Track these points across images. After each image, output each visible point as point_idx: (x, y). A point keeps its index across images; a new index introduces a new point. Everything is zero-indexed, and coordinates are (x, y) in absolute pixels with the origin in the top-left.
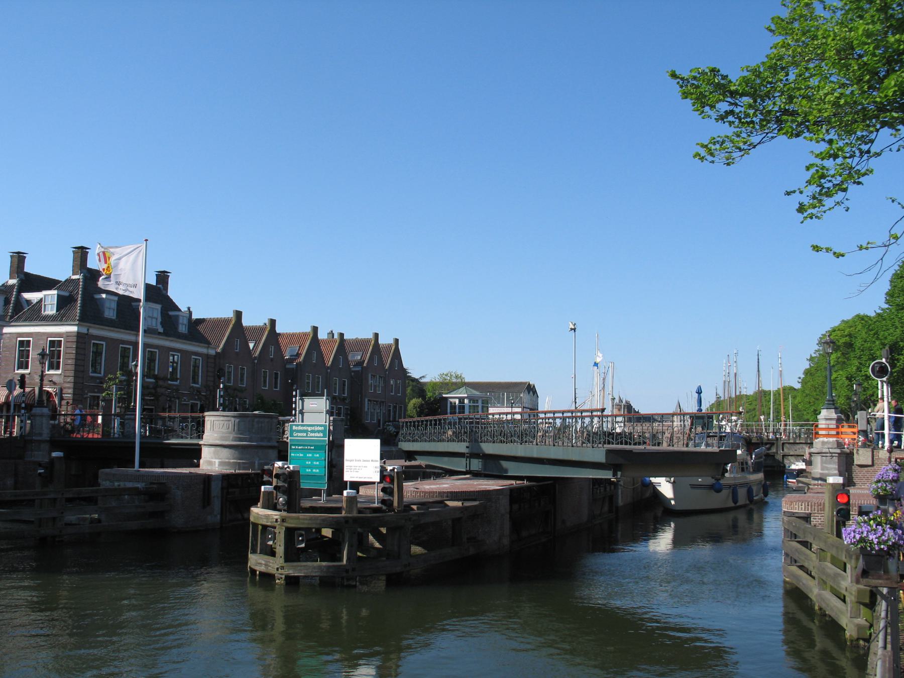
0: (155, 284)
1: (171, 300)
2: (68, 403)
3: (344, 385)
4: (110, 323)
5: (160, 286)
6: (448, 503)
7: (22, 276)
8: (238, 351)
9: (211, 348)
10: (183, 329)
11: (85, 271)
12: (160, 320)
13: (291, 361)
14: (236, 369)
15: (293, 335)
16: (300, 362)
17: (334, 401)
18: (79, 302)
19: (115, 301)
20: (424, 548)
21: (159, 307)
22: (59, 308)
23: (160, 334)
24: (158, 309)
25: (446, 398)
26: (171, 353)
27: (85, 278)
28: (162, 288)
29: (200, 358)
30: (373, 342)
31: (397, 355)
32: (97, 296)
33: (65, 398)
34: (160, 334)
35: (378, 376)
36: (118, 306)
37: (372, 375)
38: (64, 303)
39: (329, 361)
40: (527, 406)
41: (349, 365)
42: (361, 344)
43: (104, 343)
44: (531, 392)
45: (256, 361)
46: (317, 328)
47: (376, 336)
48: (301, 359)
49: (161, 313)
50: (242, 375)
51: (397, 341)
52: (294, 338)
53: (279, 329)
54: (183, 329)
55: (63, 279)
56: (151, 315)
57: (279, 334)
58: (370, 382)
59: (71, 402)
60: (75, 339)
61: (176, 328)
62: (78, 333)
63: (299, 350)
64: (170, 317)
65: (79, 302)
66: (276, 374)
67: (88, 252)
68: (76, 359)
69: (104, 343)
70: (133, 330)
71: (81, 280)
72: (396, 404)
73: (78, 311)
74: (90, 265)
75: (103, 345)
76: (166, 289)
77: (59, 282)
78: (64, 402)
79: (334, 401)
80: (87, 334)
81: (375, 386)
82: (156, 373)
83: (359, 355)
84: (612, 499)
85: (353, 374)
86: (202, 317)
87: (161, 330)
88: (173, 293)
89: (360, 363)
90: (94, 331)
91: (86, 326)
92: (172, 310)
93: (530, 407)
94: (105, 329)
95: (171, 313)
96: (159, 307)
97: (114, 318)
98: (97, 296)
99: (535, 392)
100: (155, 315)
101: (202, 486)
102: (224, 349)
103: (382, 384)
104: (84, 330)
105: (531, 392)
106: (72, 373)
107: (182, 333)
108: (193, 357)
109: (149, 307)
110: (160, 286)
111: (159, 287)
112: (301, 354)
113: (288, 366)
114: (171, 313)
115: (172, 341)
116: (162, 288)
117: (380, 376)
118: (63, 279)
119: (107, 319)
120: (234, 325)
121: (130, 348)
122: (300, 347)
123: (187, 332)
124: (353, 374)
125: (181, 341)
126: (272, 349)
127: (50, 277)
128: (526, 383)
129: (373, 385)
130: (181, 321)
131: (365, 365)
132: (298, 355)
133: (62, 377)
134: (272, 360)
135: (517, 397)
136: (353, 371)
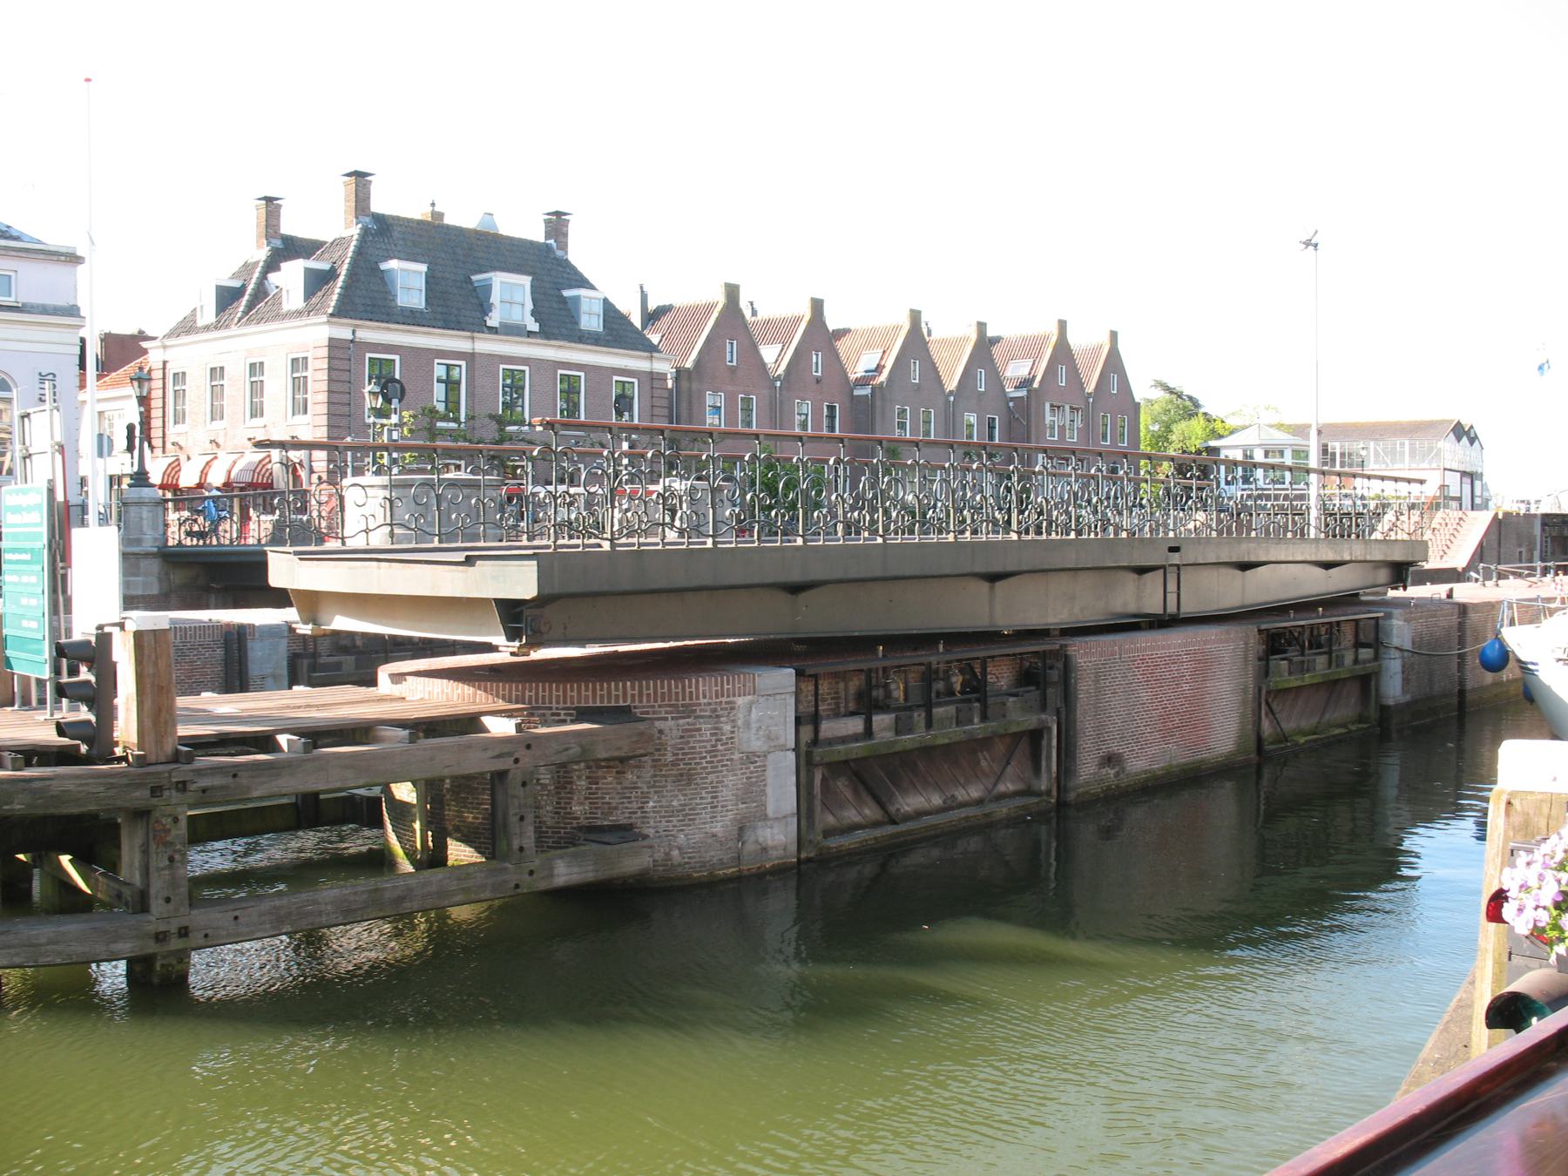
0: (542, 240)
1: (574, 269)
2: (320, 478)
3: (991, 428)
4: (411, 318)
5: (551, 241)
6: (487, 720)
7: (278, 243)
8: (917, 381)
9: (659, 359)
10: (591, 321)
11: (367, 219)
12: (529, 306)
13: (863, 382)
14: (730, 400)
15: (873, 331)
16: (882, 383)
17: (967, 460)
18: (342, 278)
19: (421, 273)
20: (478, 850)
21: (526, 281)
22: (309, 293)
23: (530, 334)
24: (523, 286)
25: (1215, 450)
26: (437, 361)
27: (365, 233)
28: (554, 245)
29: (635, 381)
30: (1054, 339)
31: (1114, 363)
32: (384, 266)
33: (315, 469)
34: (530, 334)
35: (1067, 408)
36: (427, 282)
37: (1052, 406)
38: (317, 282)
39: (951, 383)
40: (1449, 467)
41: (1003, 388)
42: (1030, 346)
43: (397, 358)
44: (1465, 439)
45: (778, 384)
46: (985, 324)
47: (1062, 325)
48: (883, 377)
49: (532, 293)
50: (831, 417)
51: (1114, 336)
52: (872, 337)
53: (832, 324)
54: (591, 321)
55: (330, 240)
56: (506, 298)
57: (841, 334)
58: (1048, 418)
59: (325, 477)
60: (324, 352)
61: (577, 323)
62: (330, 339)
63: (882, 359)
64: (564, 300)
65: (342, 278)
66: (831, 408)
67: (370, 182)
68: (330, 391)
69: (397, 358)
70: (463, 330)
71: (356, 237)
72: (1114, 463)
73: (335, 297)
74: (379, 205)
75: (394, 360)
76: (563, 246)
77: (322, 244)
78: (315, 478)
79: (967, 460)
80: (352, 341)
81: (1062, 429)
82: (500, 412)
83: (1024, 366)
84: (1367, 682)
85: (1011, 404)
86: (667, 303)
87: (534, 327)
88: (579, 254)
89: (1026, 383)
90: (371, 333)
91: (348, 325)
92: (571, 287)
93: (1462, 468)
94: (602, 352)
95: (567, 293)
96: (526, 281)
97: (423, 305)
98: (384, 266)
99: (1473, 440)
100: (518, 298)
101: (220, 652)
102: (698, 362)
103: (1078, 423)
104: (344, 333)
105: (1465, 439)
106: (324, 420)
107: (589, 332)
108: (616, 378)
109: (501, 282)
110: (551, 241)
111: (547, 245)
112: (884, 367)
113: (856, 393)
114: (567, 293)
115: (560, 347)
116: (554, 245)
117: (1071, 408)
118: (328, 237)
119: (403, 309)
120: (721, 313)
121: (394, 360)
122: (884, 352)
123: (601, 330)
124: (1011, 404)
125: (581, 346)
126: (816, 358)
127: (580, 269)
128: (1453, 421)
129: (1057, 425)
130: (584, 307)
131: (1036, 385)
132: (879, 368)
133: (311, 427)
134: (818, 381)
135: (1431, 449)
136: (1012, 399)
